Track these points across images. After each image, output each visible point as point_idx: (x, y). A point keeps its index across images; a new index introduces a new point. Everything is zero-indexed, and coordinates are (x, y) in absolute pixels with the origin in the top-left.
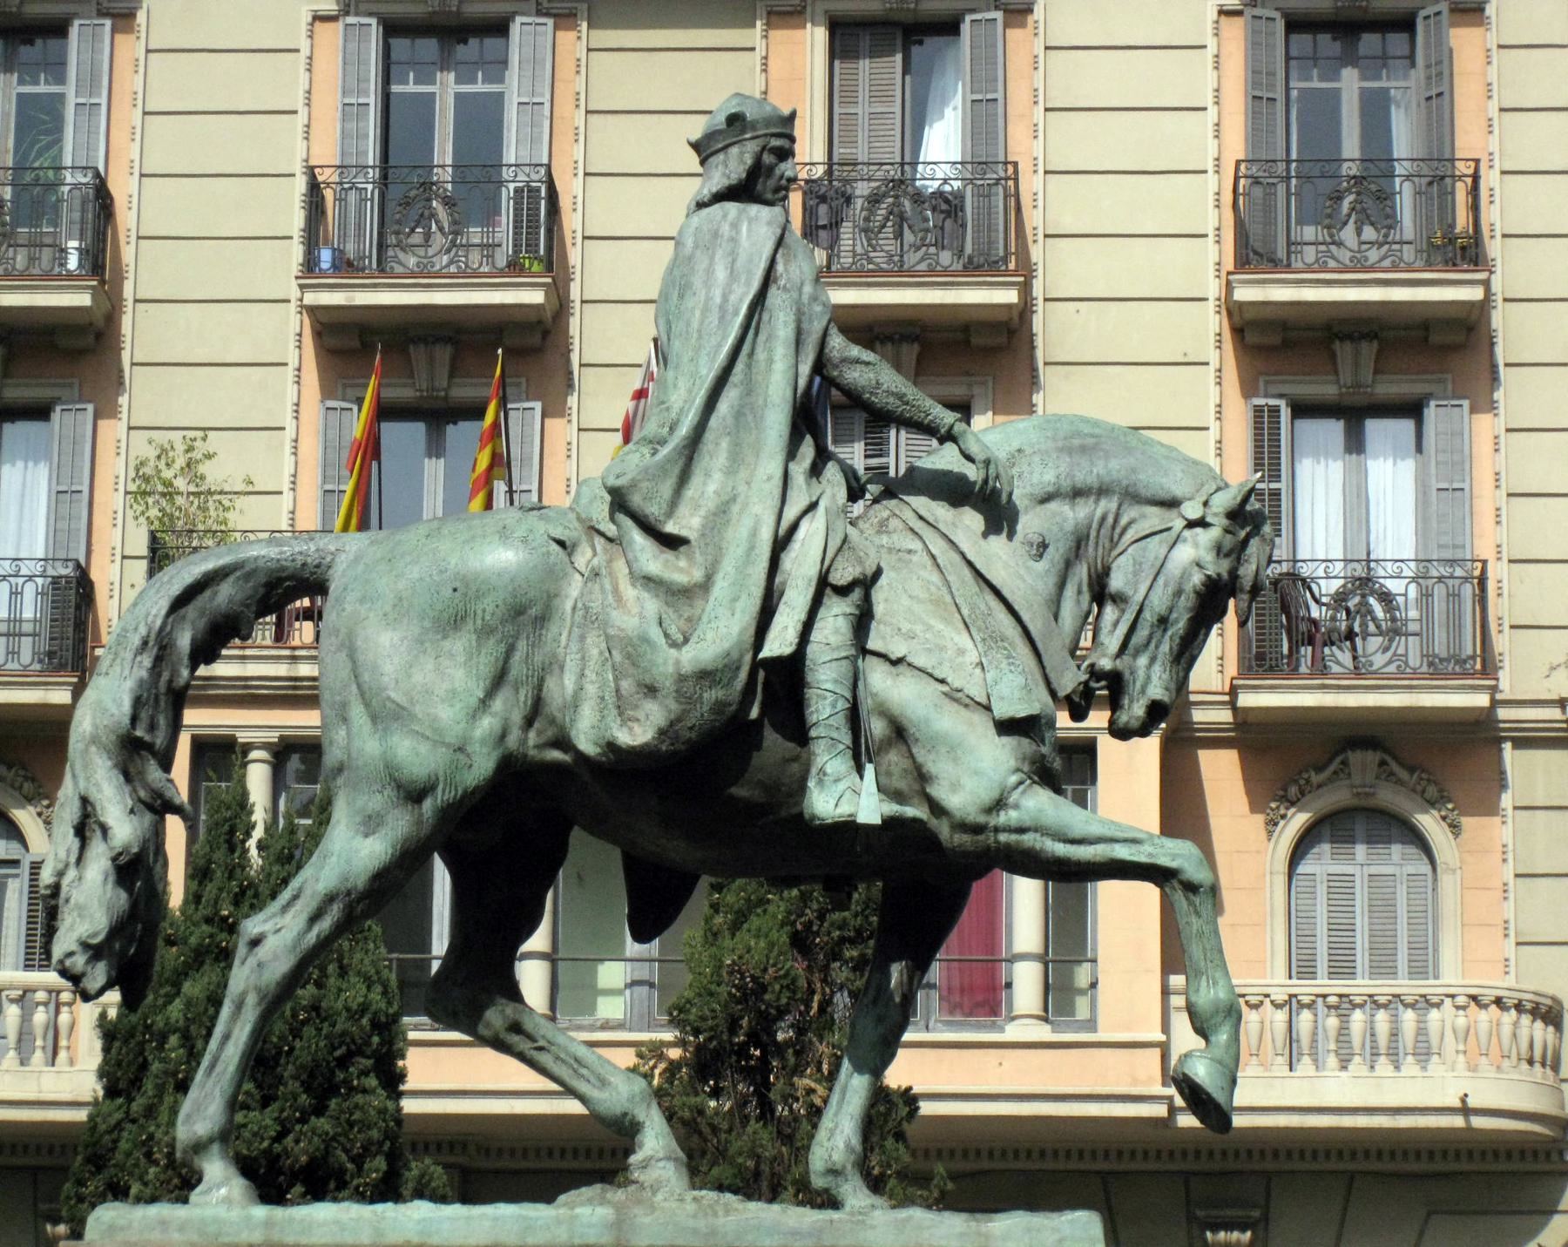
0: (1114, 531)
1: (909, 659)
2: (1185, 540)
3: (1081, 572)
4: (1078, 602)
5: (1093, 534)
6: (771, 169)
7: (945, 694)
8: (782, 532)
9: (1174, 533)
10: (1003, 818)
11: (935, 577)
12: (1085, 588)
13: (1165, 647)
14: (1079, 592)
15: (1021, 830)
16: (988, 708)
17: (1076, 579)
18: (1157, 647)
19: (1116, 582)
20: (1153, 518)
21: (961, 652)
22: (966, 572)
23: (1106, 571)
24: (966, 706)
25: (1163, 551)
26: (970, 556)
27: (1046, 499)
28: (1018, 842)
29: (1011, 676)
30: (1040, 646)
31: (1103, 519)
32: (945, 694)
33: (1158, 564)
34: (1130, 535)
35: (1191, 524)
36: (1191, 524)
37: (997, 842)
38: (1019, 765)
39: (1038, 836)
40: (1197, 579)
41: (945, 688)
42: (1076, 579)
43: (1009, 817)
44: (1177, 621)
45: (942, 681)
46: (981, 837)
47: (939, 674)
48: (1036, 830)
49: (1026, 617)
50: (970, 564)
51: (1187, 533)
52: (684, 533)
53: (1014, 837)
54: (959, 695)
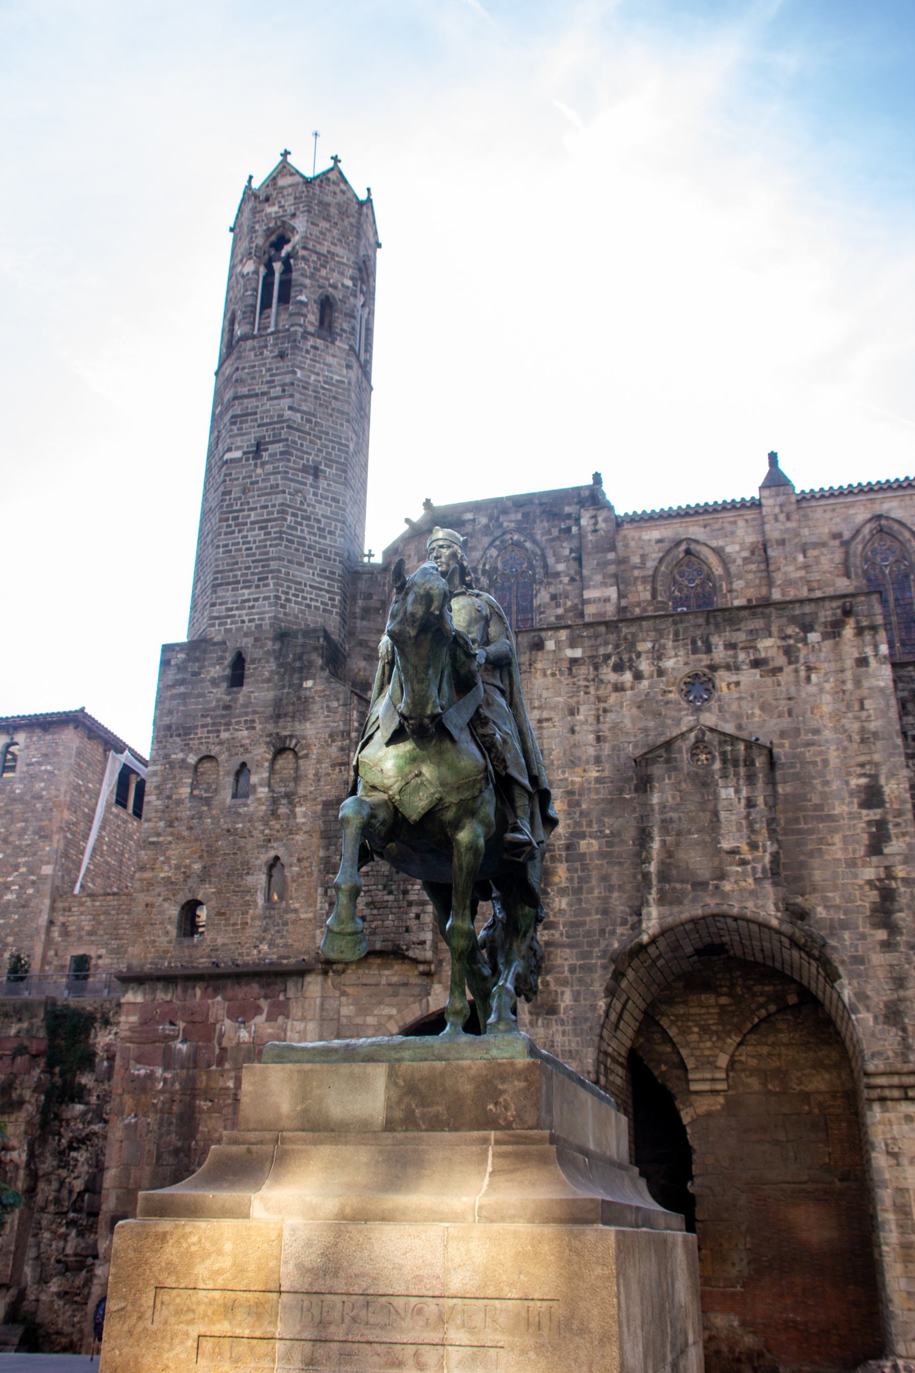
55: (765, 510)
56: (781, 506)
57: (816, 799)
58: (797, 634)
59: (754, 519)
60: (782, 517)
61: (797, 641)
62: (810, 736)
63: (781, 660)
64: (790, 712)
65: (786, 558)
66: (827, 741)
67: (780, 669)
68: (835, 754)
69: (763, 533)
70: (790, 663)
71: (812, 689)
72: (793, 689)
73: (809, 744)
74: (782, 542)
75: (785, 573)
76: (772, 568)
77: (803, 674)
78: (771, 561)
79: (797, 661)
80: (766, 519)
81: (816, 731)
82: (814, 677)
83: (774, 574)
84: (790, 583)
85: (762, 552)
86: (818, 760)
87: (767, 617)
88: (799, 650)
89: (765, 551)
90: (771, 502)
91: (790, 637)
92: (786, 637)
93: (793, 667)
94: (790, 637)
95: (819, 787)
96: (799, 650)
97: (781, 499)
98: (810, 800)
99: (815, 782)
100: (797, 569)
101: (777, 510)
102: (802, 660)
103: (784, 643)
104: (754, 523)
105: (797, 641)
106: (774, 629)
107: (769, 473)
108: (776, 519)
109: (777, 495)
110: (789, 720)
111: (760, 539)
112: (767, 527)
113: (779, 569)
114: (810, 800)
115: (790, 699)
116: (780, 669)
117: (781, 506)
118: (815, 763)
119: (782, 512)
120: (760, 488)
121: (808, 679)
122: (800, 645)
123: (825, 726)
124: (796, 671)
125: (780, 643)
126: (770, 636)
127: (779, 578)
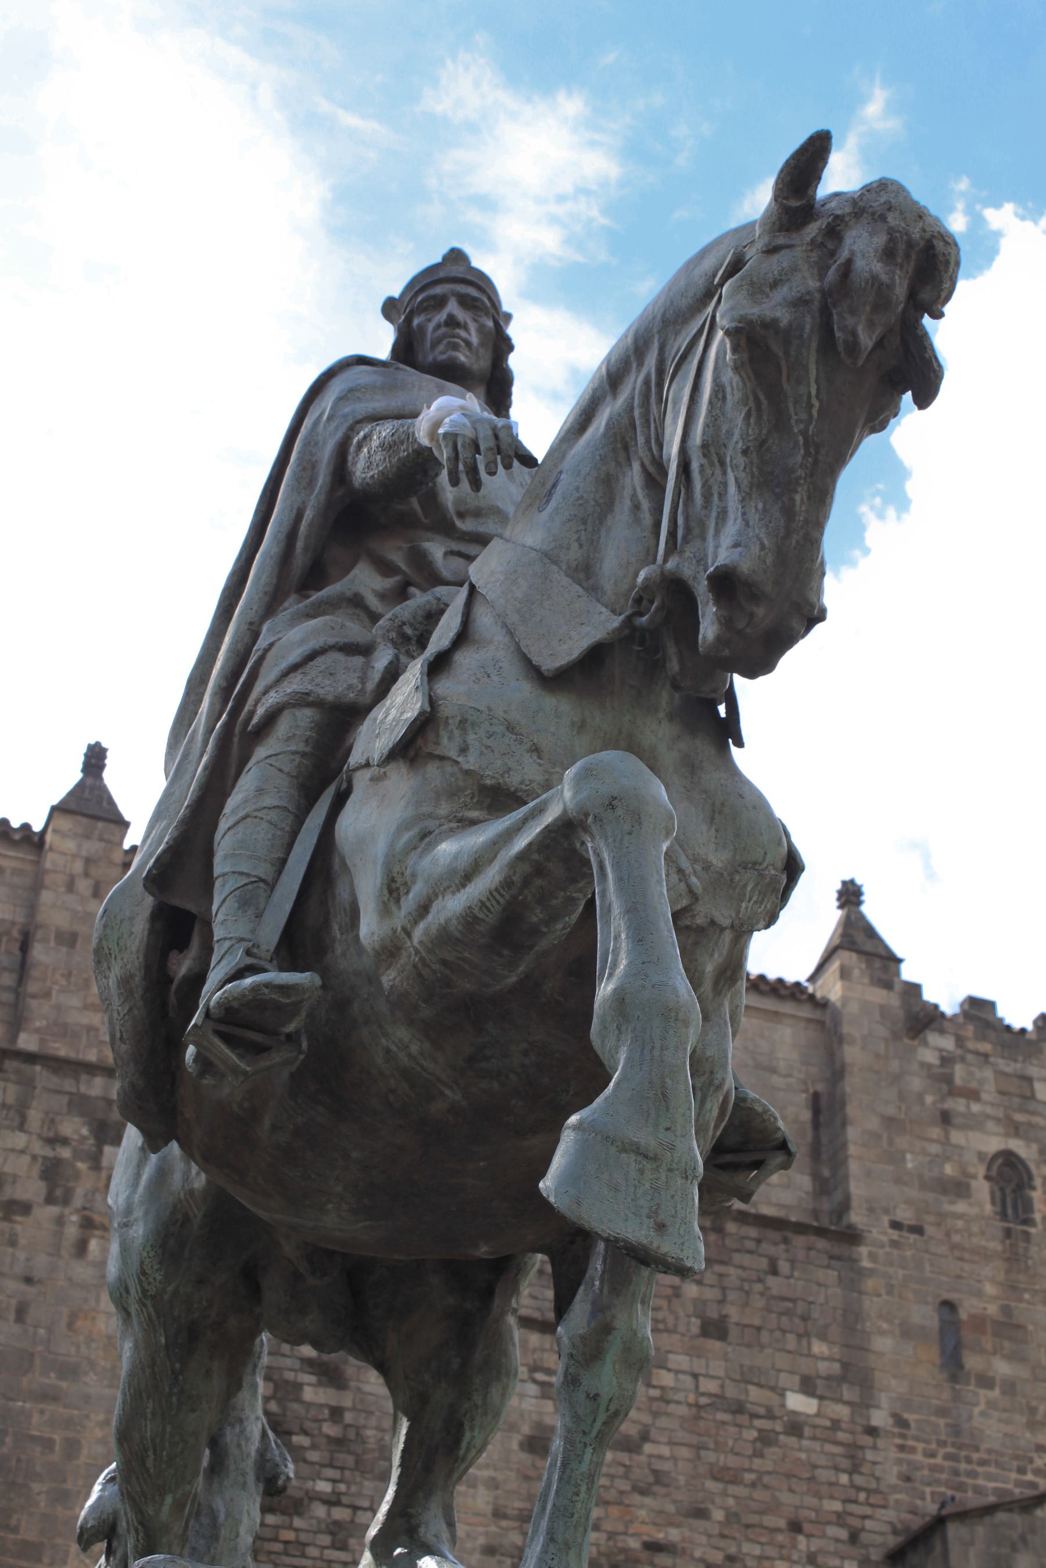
3: (634, 478)
4: (637, 520)
5: (637, 413)
6: (421, 328)
10: (410, 902)
12: (641, 494)
13: (732, 489)
14: (636, 507)
17: (627, 493)
18: (722, 496)
28: (426, 932)
31: (647, 382)
42: (627, 493)
43: (410, 902)
44: (730, 433)
46: (403, 961)
55: (50, 860)
56: (88, 861)
57: (29, 1531)
58: (83, 1139)
59: (15, 871)
60: (84, 886)
61: (77, 1155)
62: (52, 1379)
63: (32, 1189)
64: (21, 1313)
65: (68, 976)
66: (87, 1399)
67: (26, 1208)
68: (99, 1433)
69: (32, 908)
70: (50, 1200)
71: (82, 1271)
72: (41, 1261)
73: (47, 1396)
74: (69, 940)
75: (58, 1008)
76: (32, 987)
77: (72, 1231)
78: (35, 973)
79: (66, 1201)
80: (48, 879)
81: (70, 1371)
82: (93, 1245)
83: (33, 1003)
84: (64, 1031)
85: (16, 948)
86: (57, 1437)
87: (28, 1083)
88: (77, 1176)
89: (25, 947)
90: (70, 845)
91: (64, 1141)
92: (56, 1140)
93: (54, 1210)
94: (64, 1141)
95: (43, 1501)
96: (77, 1176)
97: (92, 847)
98: (15, 1530)
99: (36, 1487)
100: (86, 1007)
101: (78, 867)
102: (78, 1201)
103: (49, 1152)
104: (16, 880)
105: (77, 1155)
106: (35, 1116)
107: (80, 786)
108: (70, 887)
109: (87, 837)
110: (17, 1329)
111: (20, 919)
112: (46, 897)
113: (47, 995)
114: (15, 1530)
115: (29, 1280)
116: (26, 1208)
117: (88, 861)
118: (48, 1444)
119: (87, 874)
120: (54, 809)
121: (81, 1248)
122: (81, 1166)
123: (92, 1364)
124: (60, 1221)
125: (39, 1148)
126: (22, 1127)
127: (40, 1013)
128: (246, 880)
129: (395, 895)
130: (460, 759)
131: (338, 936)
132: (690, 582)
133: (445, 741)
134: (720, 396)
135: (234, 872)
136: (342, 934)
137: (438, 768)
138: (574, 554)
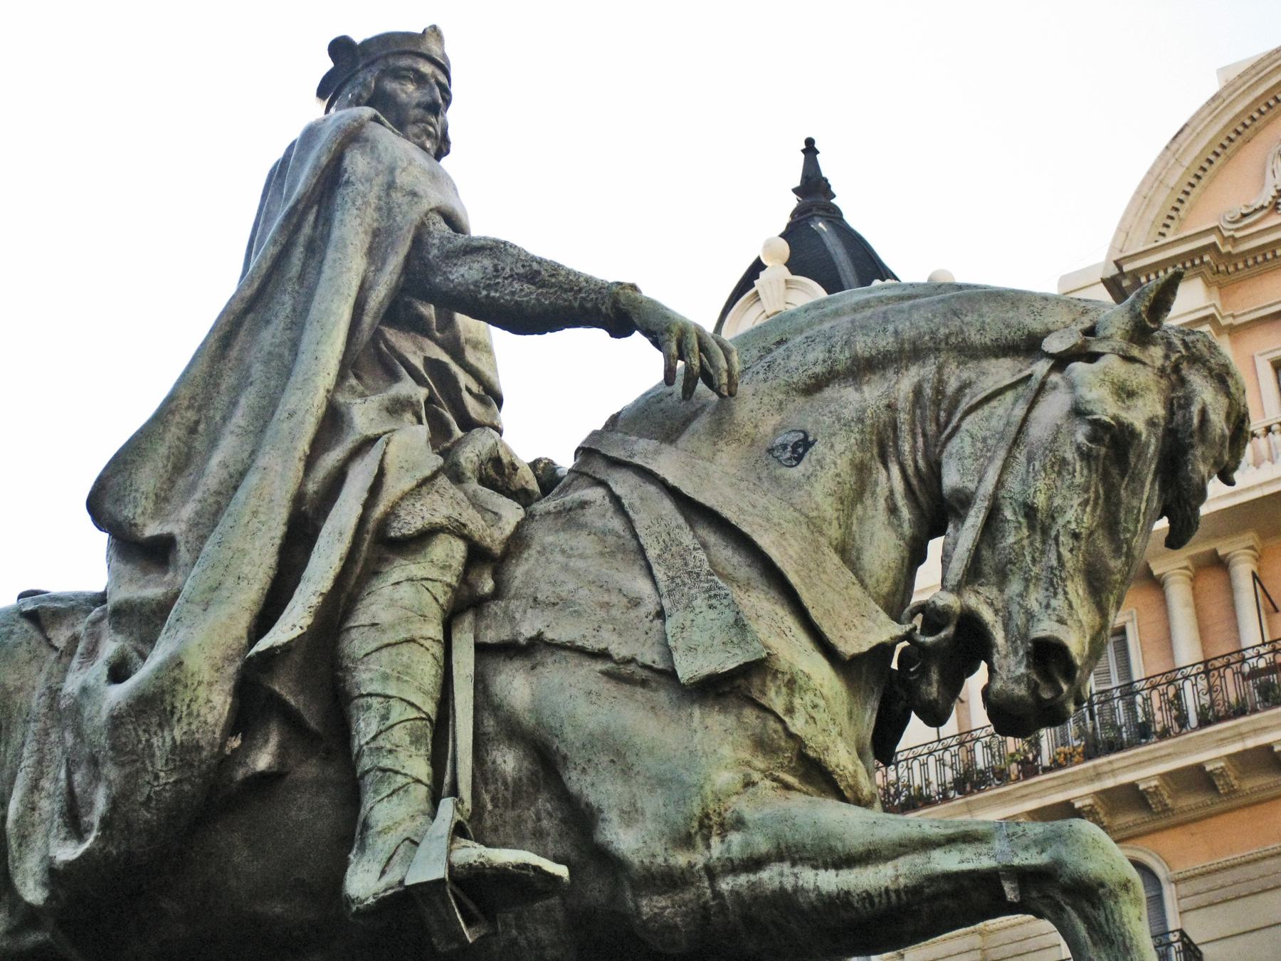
0: (940, 413)
1: (549, 635)
2: (1055, 387)
3: (890, 480)
7: (606, 674)
8: (311, 487)
9: (1034, 384)
11: (617, 524)
12: (901, 502)
14: (893, 510)
15: (755, 863)
16: (670, 675)
17: (882, 491)
19: (951, 479)
20: (1002, 371)
21: (635, 603)
22: (667, 507)
23: (935, 468)
24: (644, 683)
25: (1019, 412)
26: (671, 480)
27: (814, 386)
29: (712, 614)
30: (793, 579)
31: (918, 391)
32: (606, 674)
33: (1014, 429)
34: (964, 406)
35: (1061, 361)
36: (1061, 361)
37: (717, 895)
38: (745, 755)
39: (786, 867)
40: (1081, 434)
41: (608, 666)
45: (603, 655)
47: (592, 644)
48: (781, 859)
49: (765, 541)
50: (674, 493)
51: (1055, 378)
52: (166, 529)
53: (743, 879)
54: (632, 667)
128: (415, 714)
129: (705, 831)
130: (787, 719)
131: (490, 807)
132: (990, 627)
133: (772, 694)
134: (1056, 469)
135: (402, 699)
136: (495, 806)
137: (758, 717)
138: (834, 532)
